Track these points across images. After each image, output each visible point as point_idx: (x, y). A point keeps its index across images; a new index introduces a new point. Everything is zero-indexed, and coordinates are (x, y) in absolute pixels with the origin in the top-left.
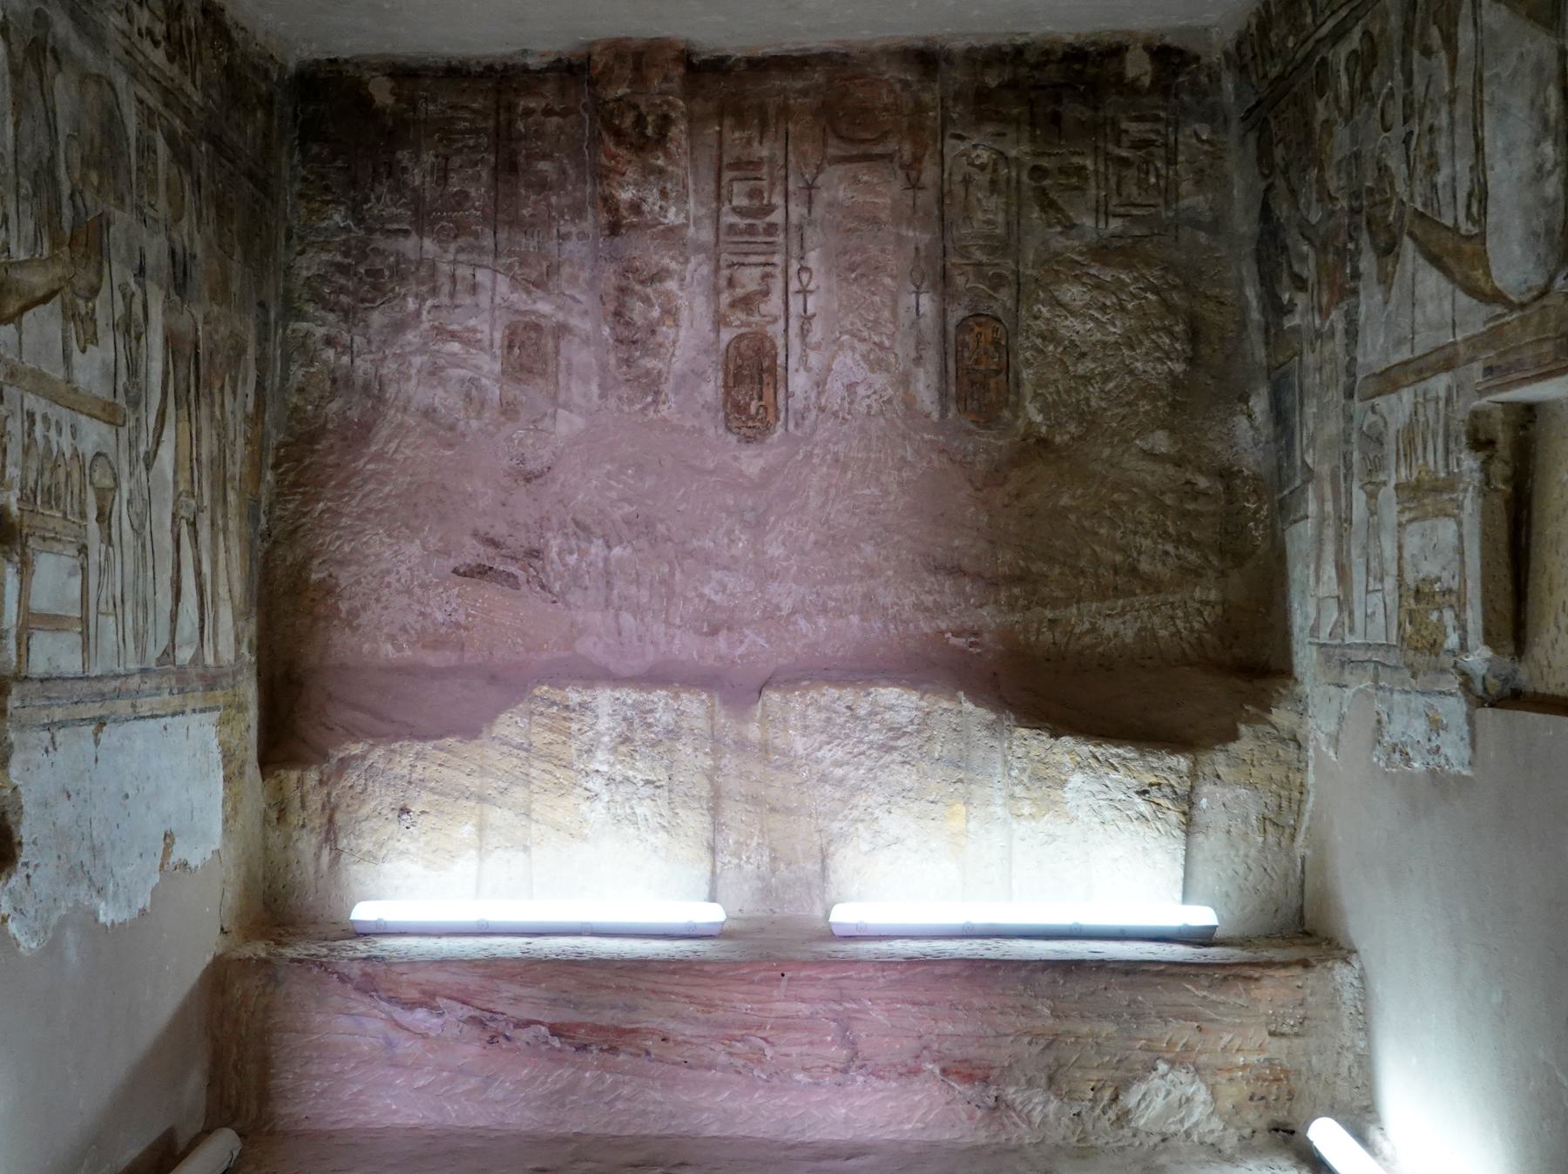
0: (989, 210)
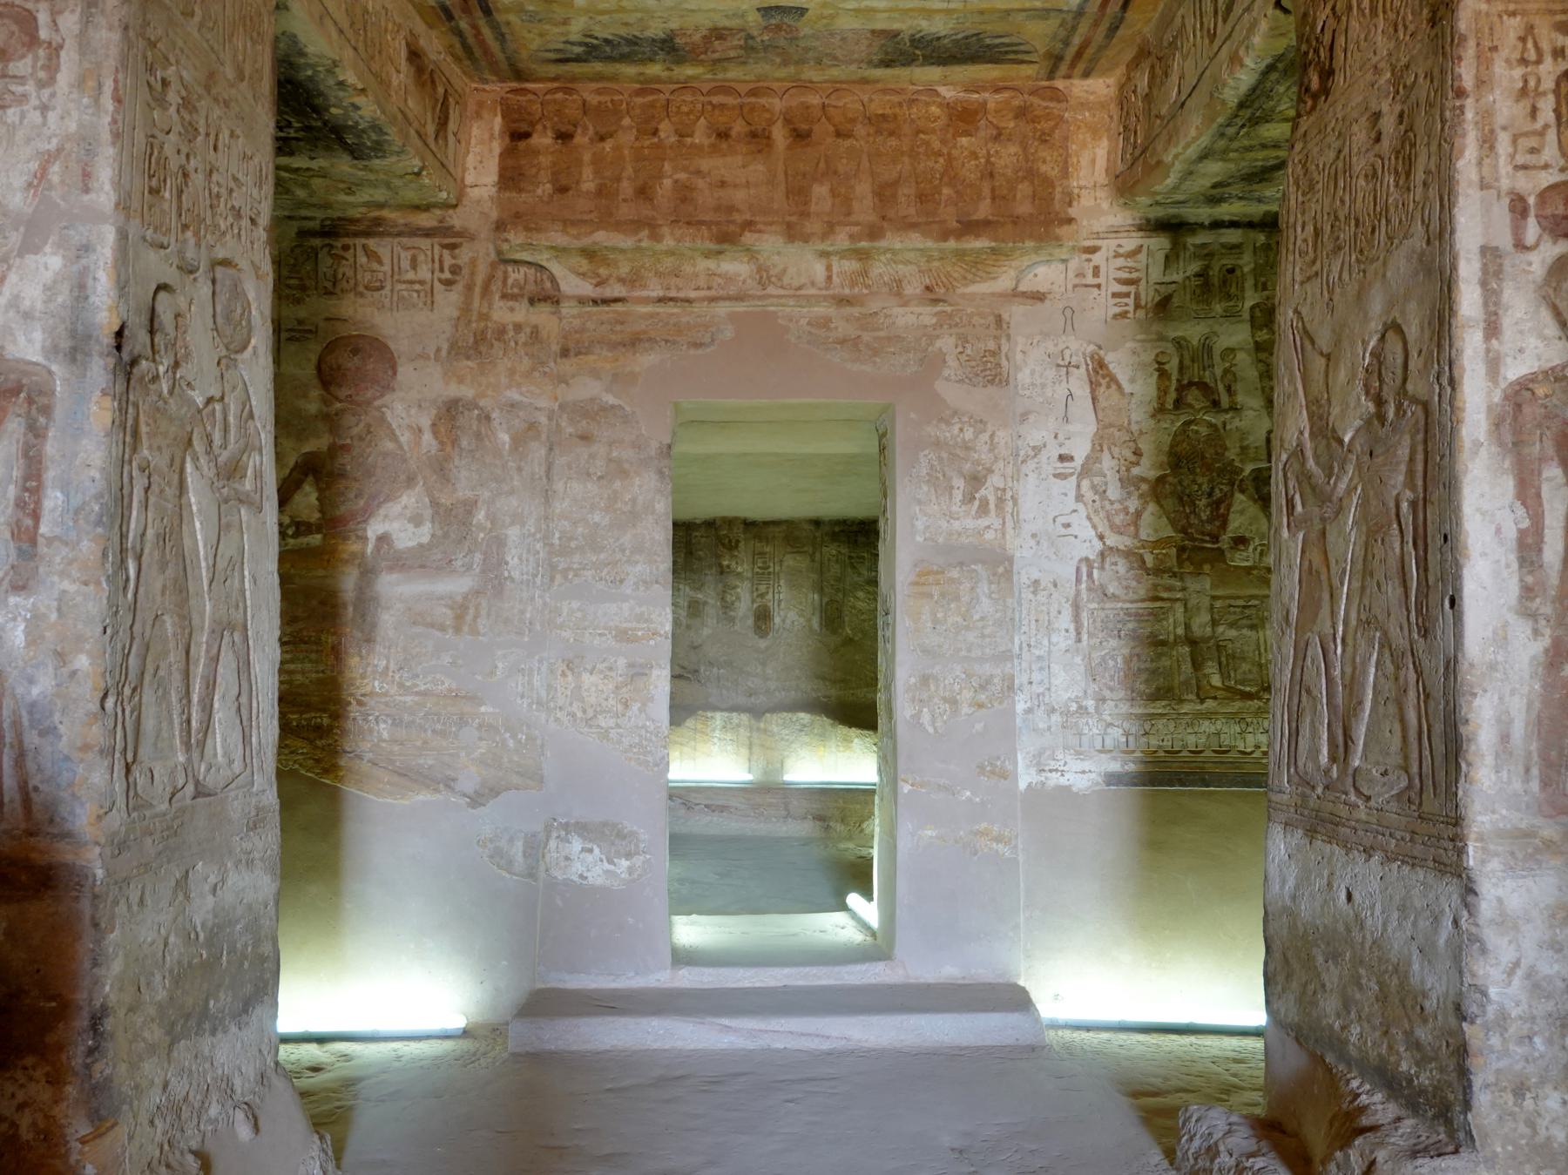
0: (835, 569)
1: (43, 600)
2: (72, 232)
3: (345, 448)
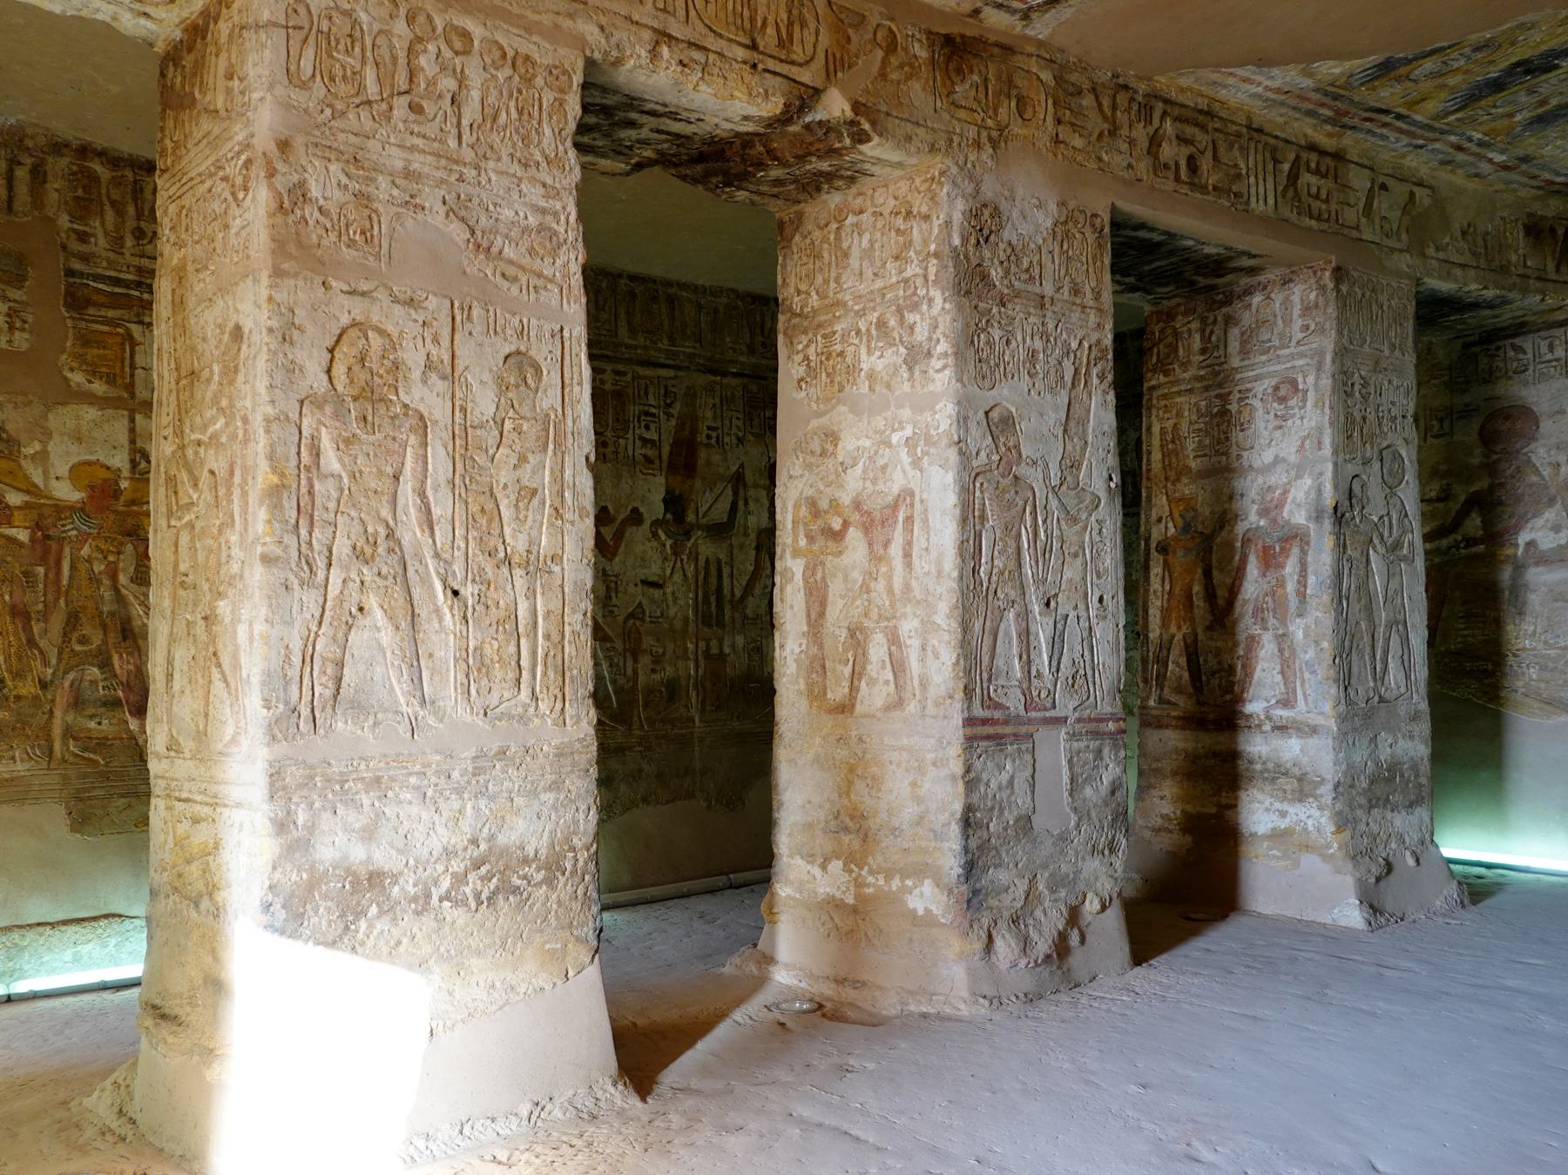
1: (1309, 620)
3: (1501, 485)
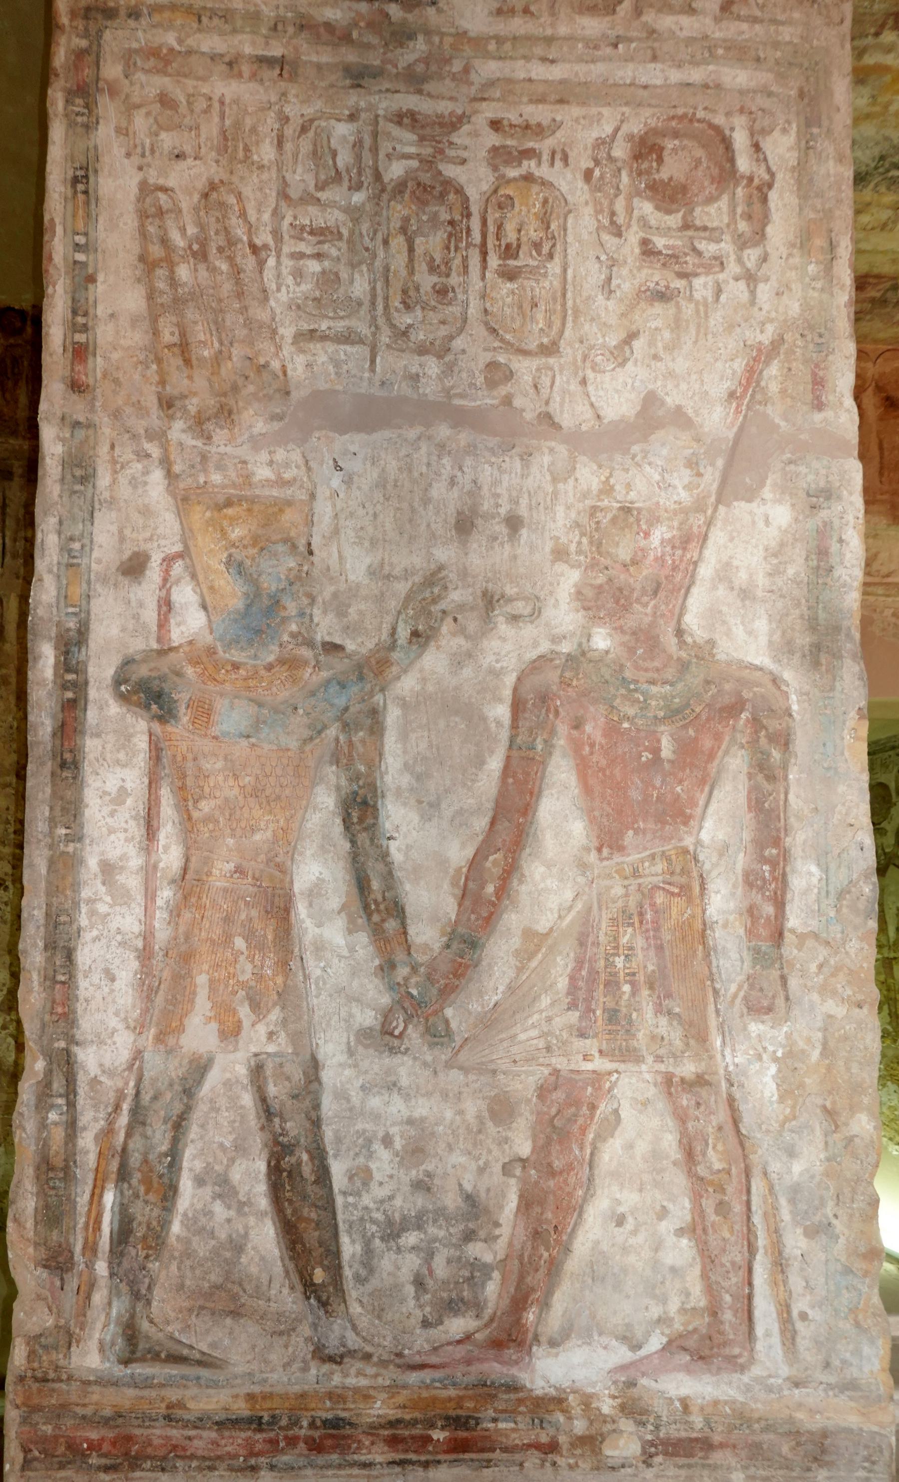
2: (803, 469)
